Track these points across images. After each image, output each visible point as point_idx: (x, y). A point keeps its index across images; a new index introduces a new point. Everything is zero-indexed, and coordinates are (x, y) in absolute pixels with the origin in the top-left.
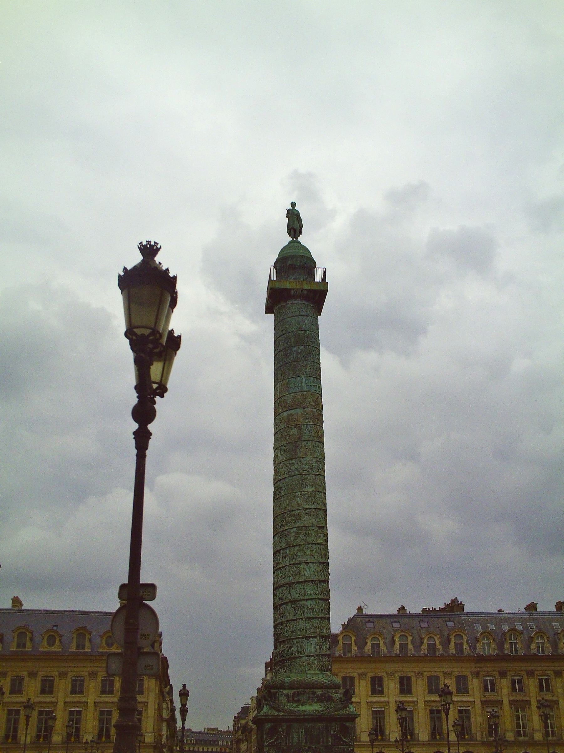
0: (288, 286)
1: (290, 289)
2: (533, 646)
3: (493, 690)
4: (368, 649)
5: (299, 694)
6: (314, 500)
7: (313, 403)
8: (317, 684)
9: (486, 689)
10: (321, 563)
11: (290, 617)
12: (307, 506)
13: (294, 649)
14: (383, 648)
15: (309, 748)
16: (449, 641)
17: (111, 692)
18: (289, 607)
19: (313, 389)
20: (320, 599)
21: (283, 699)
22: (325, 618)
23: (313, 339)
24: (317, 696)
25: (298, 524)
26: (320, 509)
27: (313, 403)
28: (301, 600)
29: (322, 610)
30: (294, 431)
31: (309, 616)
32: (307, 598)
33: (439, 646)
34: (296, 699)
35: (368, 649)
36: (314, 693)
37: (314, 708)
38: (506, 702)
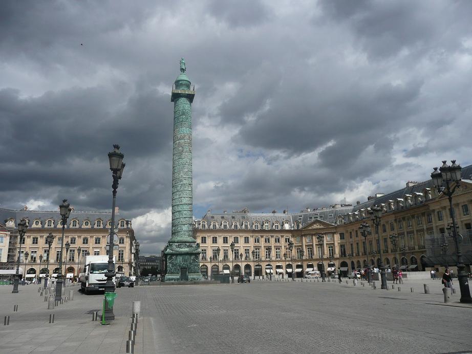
0: (180, 92)
2: (274, 226)
3: (258, 242)
4: (211, 227)
5: (180, 245)
9: (256, 242)
11: (178, 217)
13: (179, 229)
14: (217, 226)
16: (242, 224)
18: (177, 213)
19: (188, 132)
21: (174, 247)
25: (181, 183)
30: (181, 148)
33: (238, 226)
35: (211, 227)
37: (186, 250)
38: (263, 247)
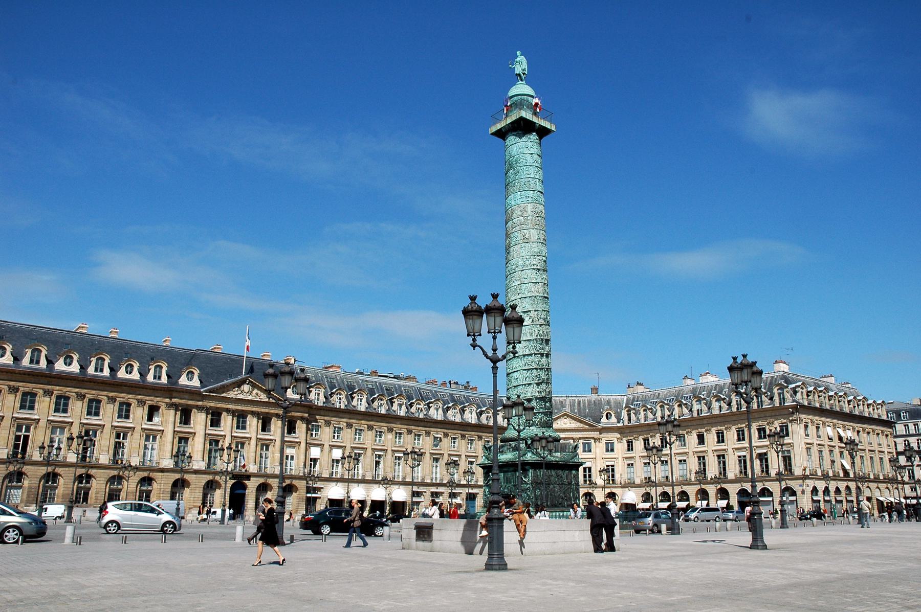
1: (501, 129)
6: (519, 291)
7: (520, 213)
8: (514, 438)
10: (525, 340)
12: (514, 298)
15: (505, 486)
17: (744, 439)
20: (523, 370)
22: (530, 384)
23: (521, 160)
24: (512, 448)
26: (526, 298)
27: (520, 213)
28: (510, 373)
29: (526, 378)
31: (515, 385)
32: (514, 370)
34: (501, 450)
36: (510, 445)
